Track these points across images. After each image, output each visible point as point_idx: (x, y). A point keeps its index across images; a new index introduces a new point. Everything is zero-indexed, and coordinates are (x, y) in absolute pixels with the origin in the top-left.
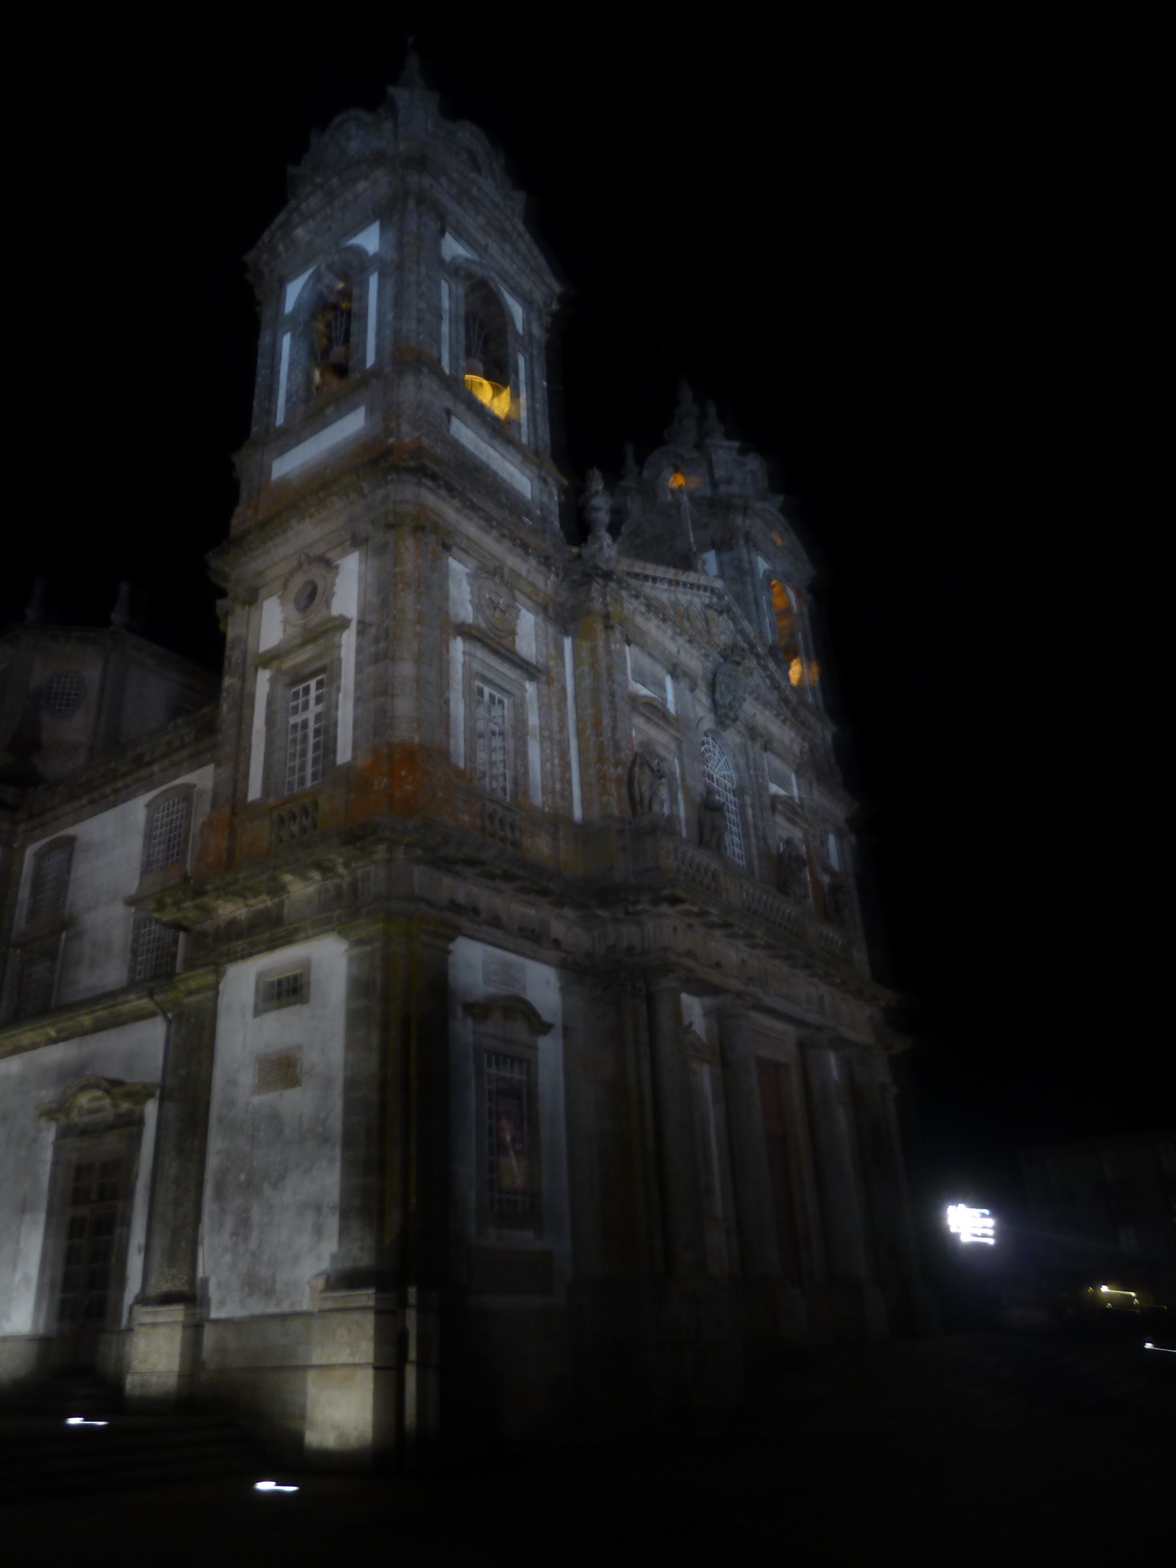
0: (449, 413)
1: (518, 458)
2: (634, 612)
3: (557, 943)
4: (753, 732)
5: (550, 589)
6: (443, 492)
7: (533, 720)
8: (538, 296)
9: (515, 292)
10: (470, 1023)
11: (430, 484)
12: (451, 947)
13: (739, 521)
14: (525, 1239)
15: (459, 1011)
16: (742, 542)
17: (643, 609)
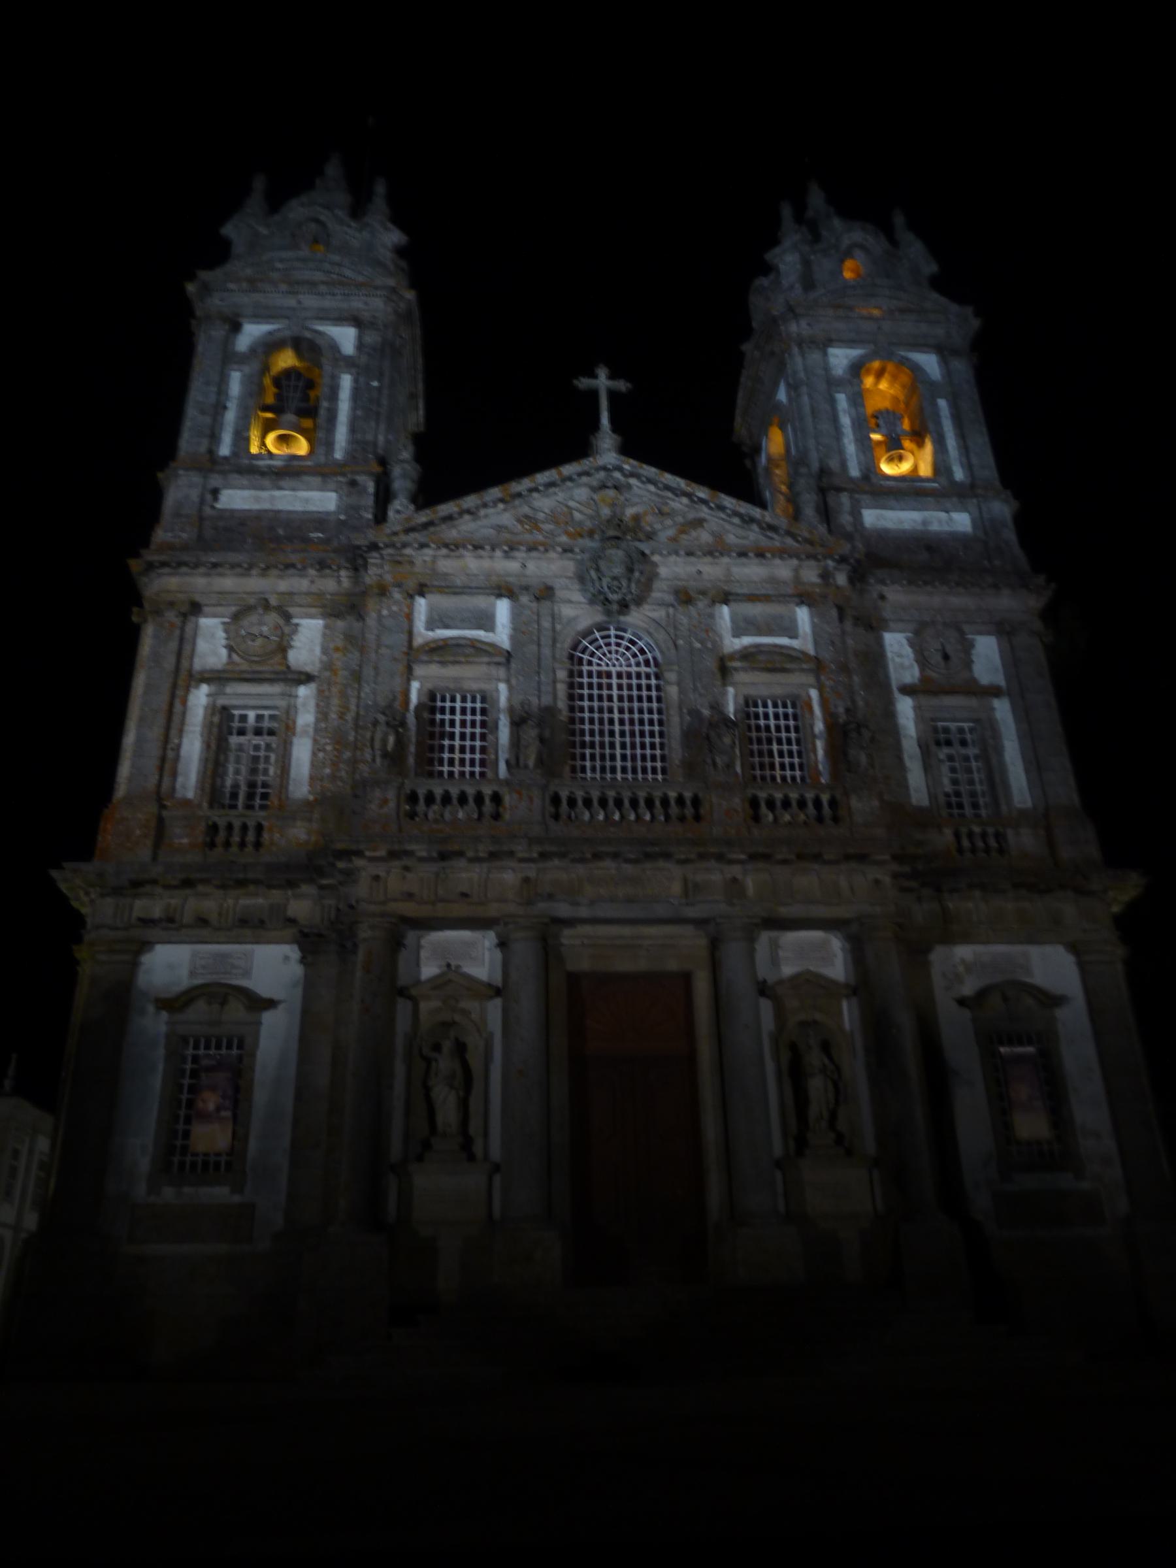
0: (215, 493)
1: (317, 480)
2: (434, 562)
3: (292, 921)
4: (684, 597)
5: (346, 583)
6: (184, 569)
7: (306, 718)
8: (376, 305)
9: (341, 319)
10: (164, 1015)
11: (166, 570)
13: (793, 328)
14: (220, 1193)
15: (151, 1008)
16: (795, 350)
17: (444, 551)
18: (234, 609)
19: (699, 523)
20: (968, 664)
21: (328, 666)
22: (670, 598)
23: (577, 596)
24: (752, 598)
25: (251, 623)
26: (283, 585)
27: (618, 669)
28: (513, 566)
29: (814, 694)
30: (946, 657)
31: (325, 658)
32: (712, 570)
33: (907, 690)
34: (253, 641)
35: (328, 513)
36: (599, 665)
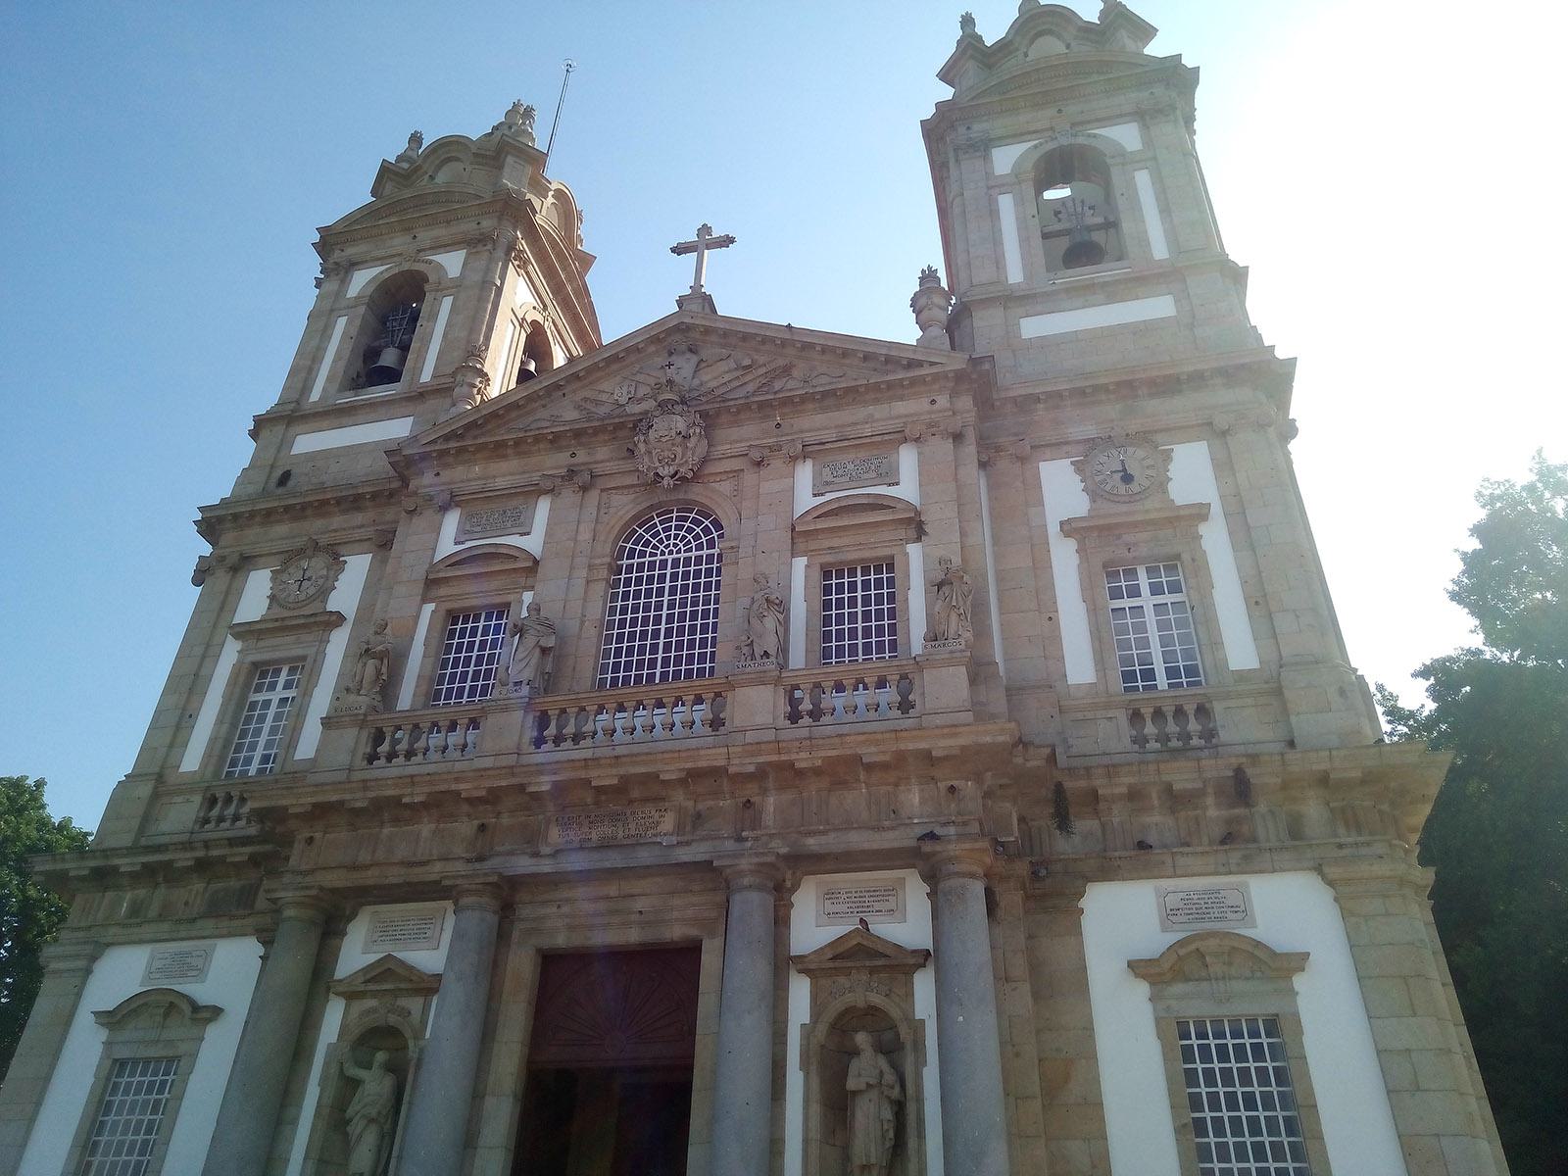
20: (1162, 485)
27: (675, 556)
30: (1127, 478)
36: (652, 555)
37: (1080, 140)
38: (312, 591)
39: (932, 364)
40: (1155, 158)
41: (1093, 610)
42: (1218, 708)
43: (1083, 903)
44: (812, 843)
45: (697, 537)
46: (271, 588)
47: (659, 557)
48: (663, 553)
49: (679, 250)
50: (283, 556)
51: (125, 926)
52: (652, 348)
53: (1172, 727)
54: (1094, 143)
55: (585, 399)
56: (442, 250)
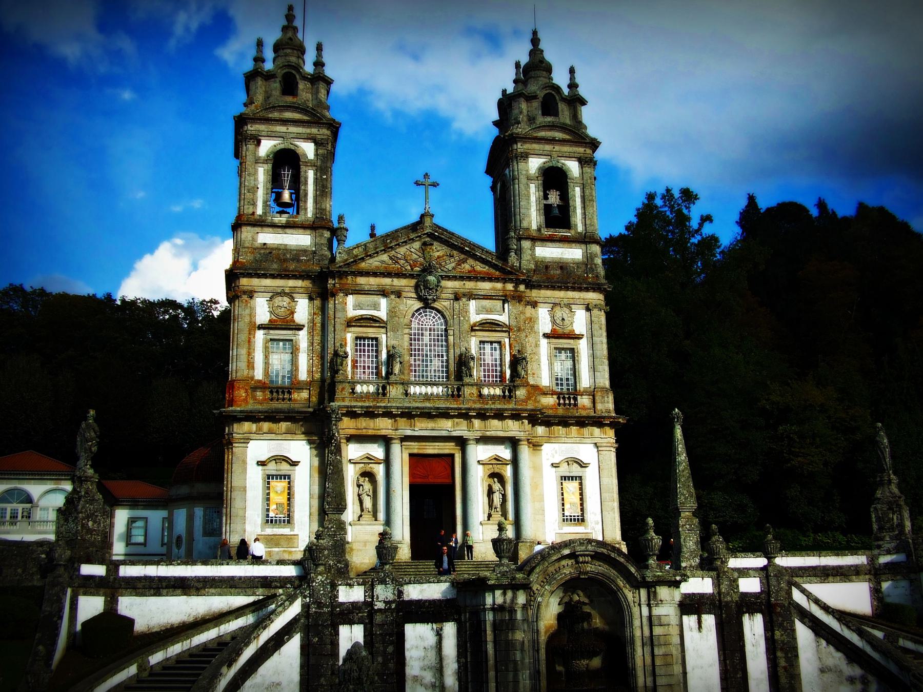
1: (301, 231)
12: (248, 445)
18: (271, 294)
19: (464, 261)
21: (312, 321)
22: (452, 296)
23: (414, 295)
24: (486, 297)
25: (278, 301)
26: (291, 283)
28: (387, 281)
29: (507, 340)
30: (563, 319)
31: (310, 318)
32: (470, 285)
33: (546, 336)
34: (280, 309)
35: (307, 246)
36: (422, 325)
37: (559, 165)
38: (288, 312)
39: (516, 274)
40: (583, 184)
41: (551, 364)
42: (579, 397)
43: (543, 447)
44: (488, 434)
45: (436, 321)
46: (269, 307)
47: (424, 326)
48: (425, 325)
49: (417, 183)
50: (271, 294)
51: (258, 434)
52: (417, 239)
53: (567, 402)
54: (564, 168)
55: (393, 256)
56: (302, 140)
